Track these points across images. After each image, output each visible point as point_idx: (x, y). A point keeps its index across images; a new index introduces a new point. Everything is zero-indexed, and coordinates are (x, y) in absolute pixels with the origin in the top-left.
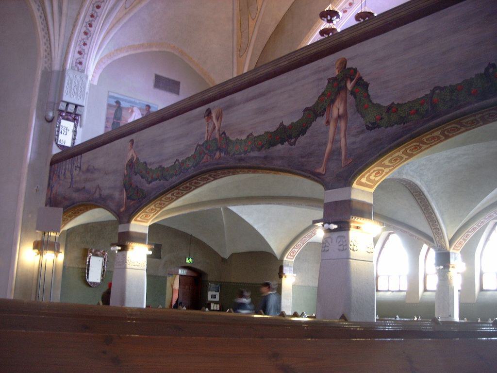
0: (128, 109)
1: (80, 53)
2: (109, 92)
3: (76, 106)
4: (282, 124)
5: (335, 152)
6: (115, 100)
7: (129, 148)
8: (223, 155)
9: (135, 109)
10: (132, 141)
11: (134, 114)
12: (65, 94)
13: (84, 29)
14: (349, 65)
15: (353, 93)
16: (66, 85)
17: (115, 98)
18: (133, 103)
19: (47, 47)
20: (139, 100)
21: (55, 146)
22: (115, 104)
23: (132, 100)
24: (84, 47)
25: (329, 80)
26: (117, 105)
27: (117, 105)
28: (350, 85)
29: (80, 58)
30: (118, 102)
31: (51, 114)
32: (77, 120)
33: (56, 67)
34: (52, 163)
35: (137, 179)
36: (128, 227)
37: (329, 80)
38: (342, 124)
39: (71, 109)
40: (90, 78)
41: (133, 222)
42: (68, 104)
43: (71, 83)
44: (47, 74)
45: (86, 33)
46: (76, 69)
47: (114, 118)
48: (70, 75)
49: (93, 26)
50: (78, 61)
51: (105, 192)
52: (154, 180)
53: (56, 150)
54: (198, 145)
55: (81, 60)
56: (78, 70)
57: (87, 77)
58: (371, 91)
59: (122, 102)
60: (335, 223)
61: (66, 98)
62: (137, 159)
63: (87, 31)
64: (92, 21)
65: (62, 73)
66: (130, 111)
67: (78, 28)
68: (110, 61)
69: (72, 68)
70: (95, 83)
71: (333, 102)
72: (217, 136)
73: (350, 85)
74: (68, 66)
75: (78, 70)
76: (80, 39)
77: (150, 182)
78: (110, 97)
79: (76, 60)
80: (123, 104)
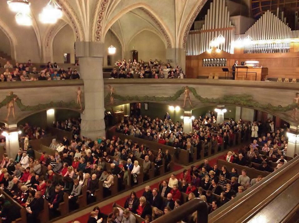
14: (14, 94)
15: (16, 101)
25: (7, 96)
28: (15, 99)
37: (7, 96)
38: (13, 109)
58: (22, 102)
71: (9, 102)
73: (15, 99)
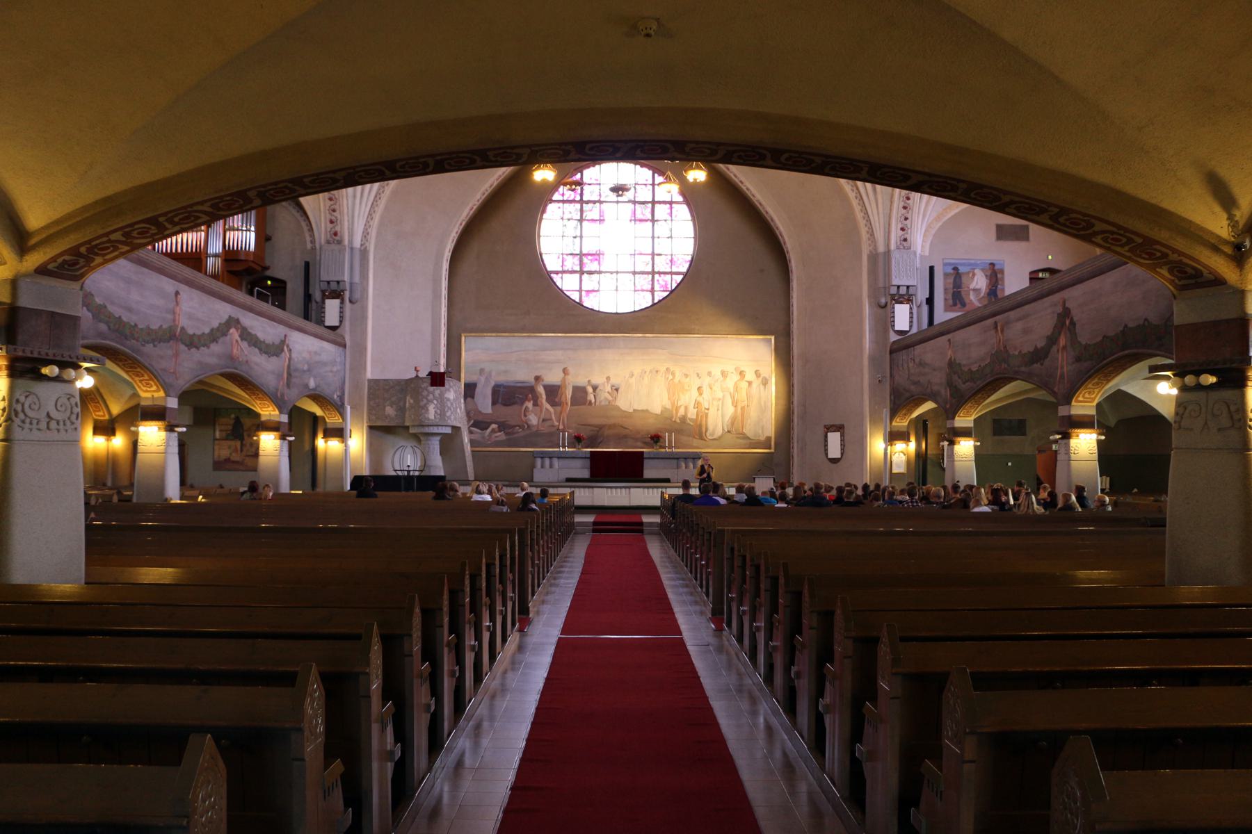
0: (968, 273)
1: (902, 229)
2: (943, 259)
3: (908, 287)
4: (1036, 347)
5: (1062, 376)
6: (952, 267)
7: (948, 347)
8: (1006, 366)
9: (977, 271)
10: (949, 340)
11: (976, 278)
12: (894, 277)
13: (902, 204)
16: (893, 267)
17: (950, 264)
18: (974, 266)
19: (869, 228)
20: (980, 260)
21: (892, 333)
22: (952, 271)
23: (973, 262)
24: (906, 222)
26: (955, 272)
27: (955, 272)
29: (903, 235)
30: (956, 269)
31: (883, 301)
32: (912, 301)
33: (881, 249)
34: (891, 353)
35: (955, 378)
36: (953, 424)
39: (903, 291)
40: (919, 252)
41: (957, 418)
42: (899, 287)
43: (899, 264)
44: (873, 257)
45: (905, 208)
46: (902, 247)
47: (954, 288)
48: (896, 256)
49: (911, 198)
50: (902, 238)
51: (935, 388)
52: (967, 381)
53: (894, 337)
54: (992, 354)
55: (906, 236)
56: (904, 247)
57: (915, 253)
59: (960, 268)
60: (1059, 434)
61: (895, 282)
62: (954, 359)
63: (906, 205)
64: (908, 194)
65: (888, 253)
66: (971, 275)
67: (895, 205)
68: (940, 224)
69: (898, 248)
70: (927, 253)
72: (1002, 349)
74: (893, 247)
75: (904, 247)
76: (900, 215)
77: (964, 383)
78: (945, 265)
79: (900, 237)
80: (962, 269)
